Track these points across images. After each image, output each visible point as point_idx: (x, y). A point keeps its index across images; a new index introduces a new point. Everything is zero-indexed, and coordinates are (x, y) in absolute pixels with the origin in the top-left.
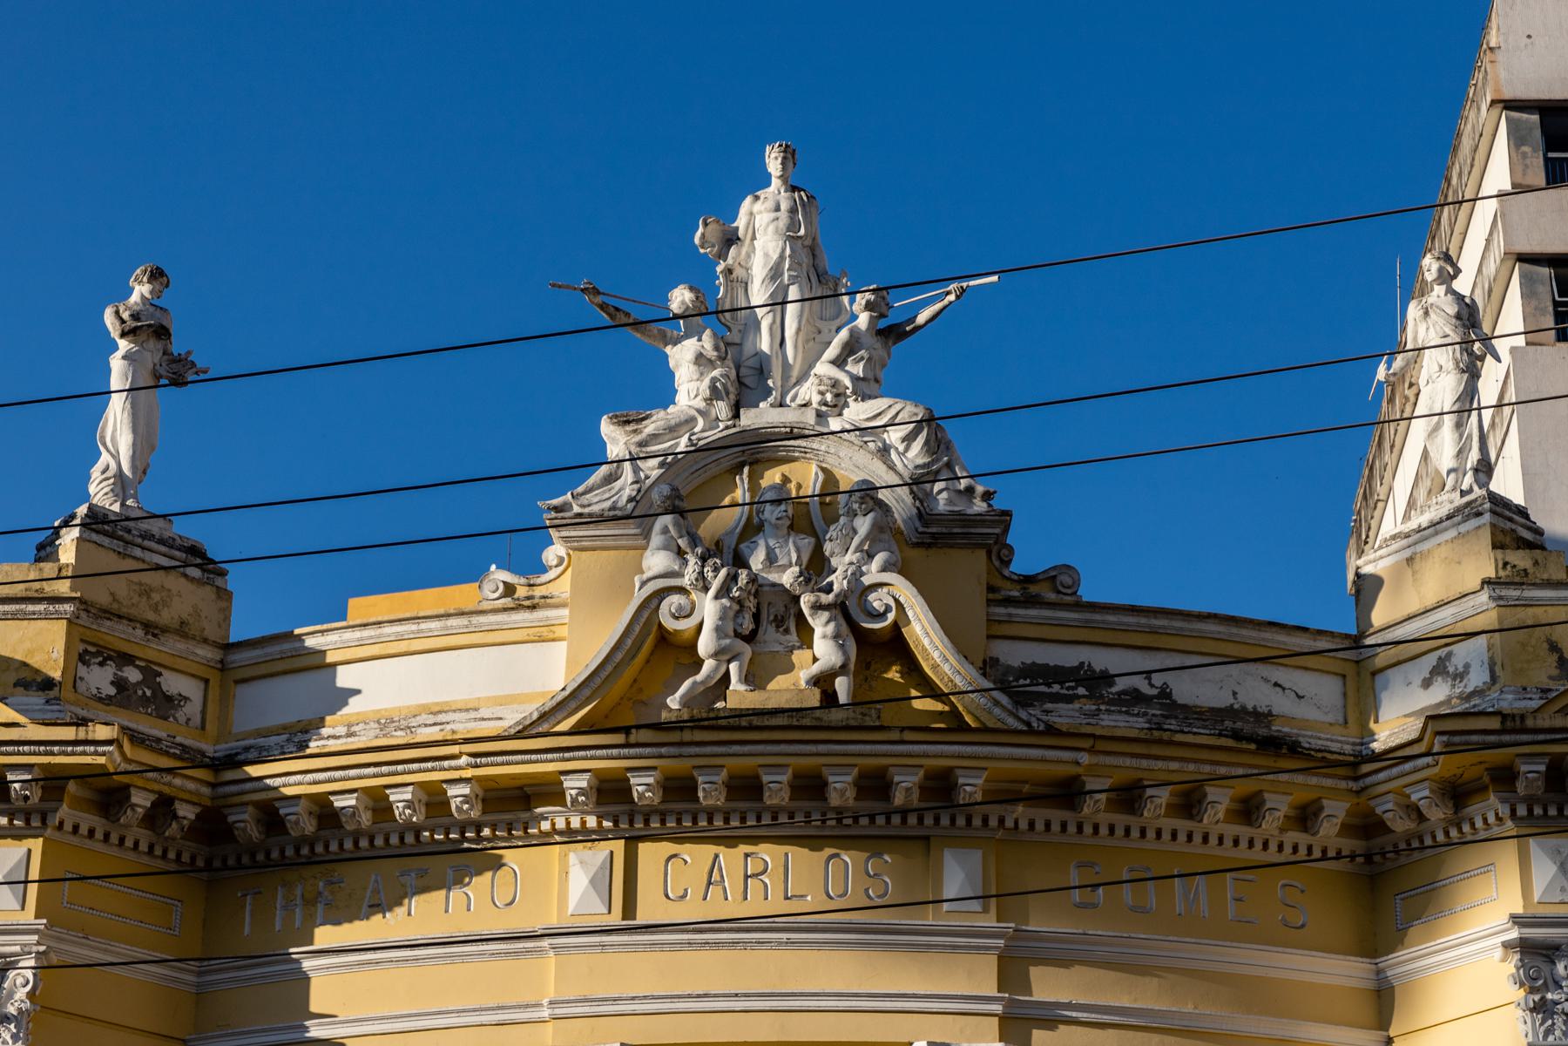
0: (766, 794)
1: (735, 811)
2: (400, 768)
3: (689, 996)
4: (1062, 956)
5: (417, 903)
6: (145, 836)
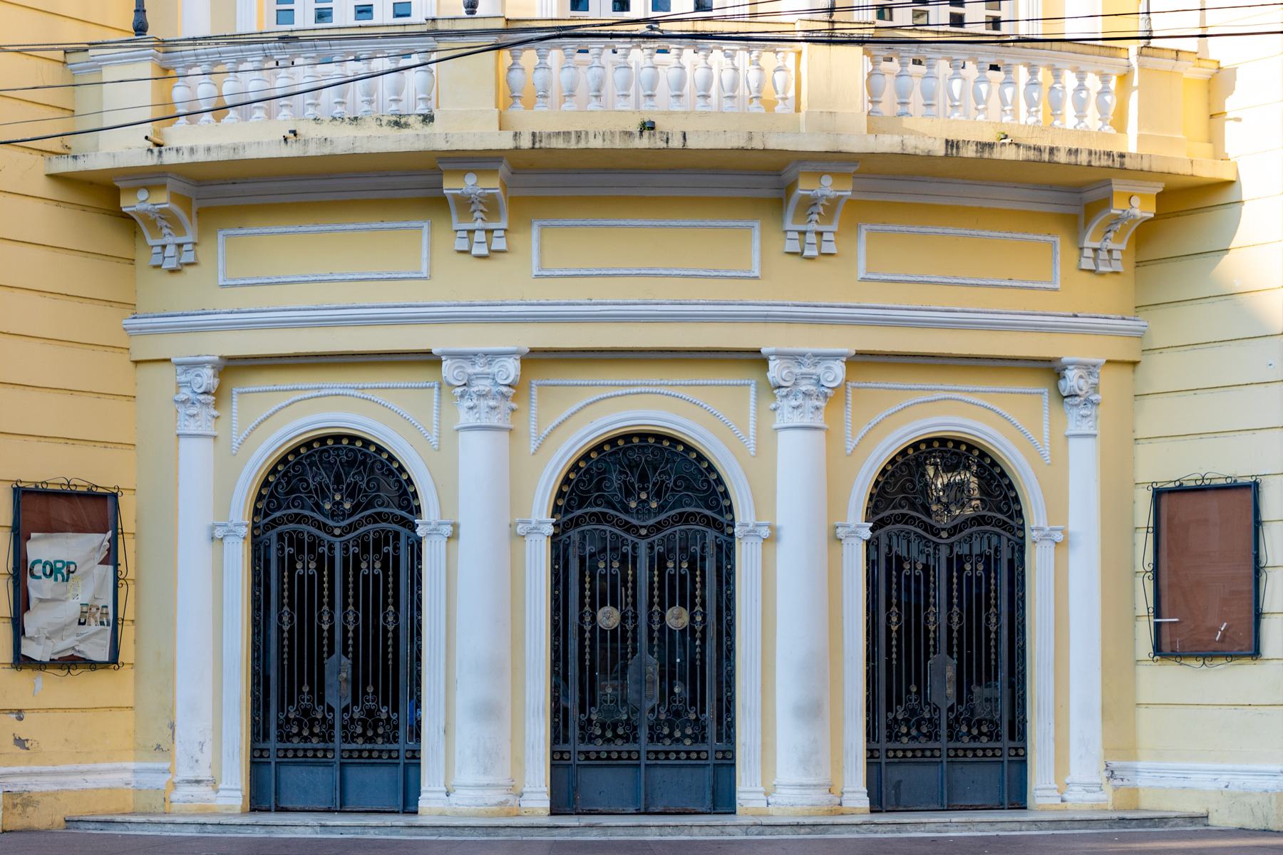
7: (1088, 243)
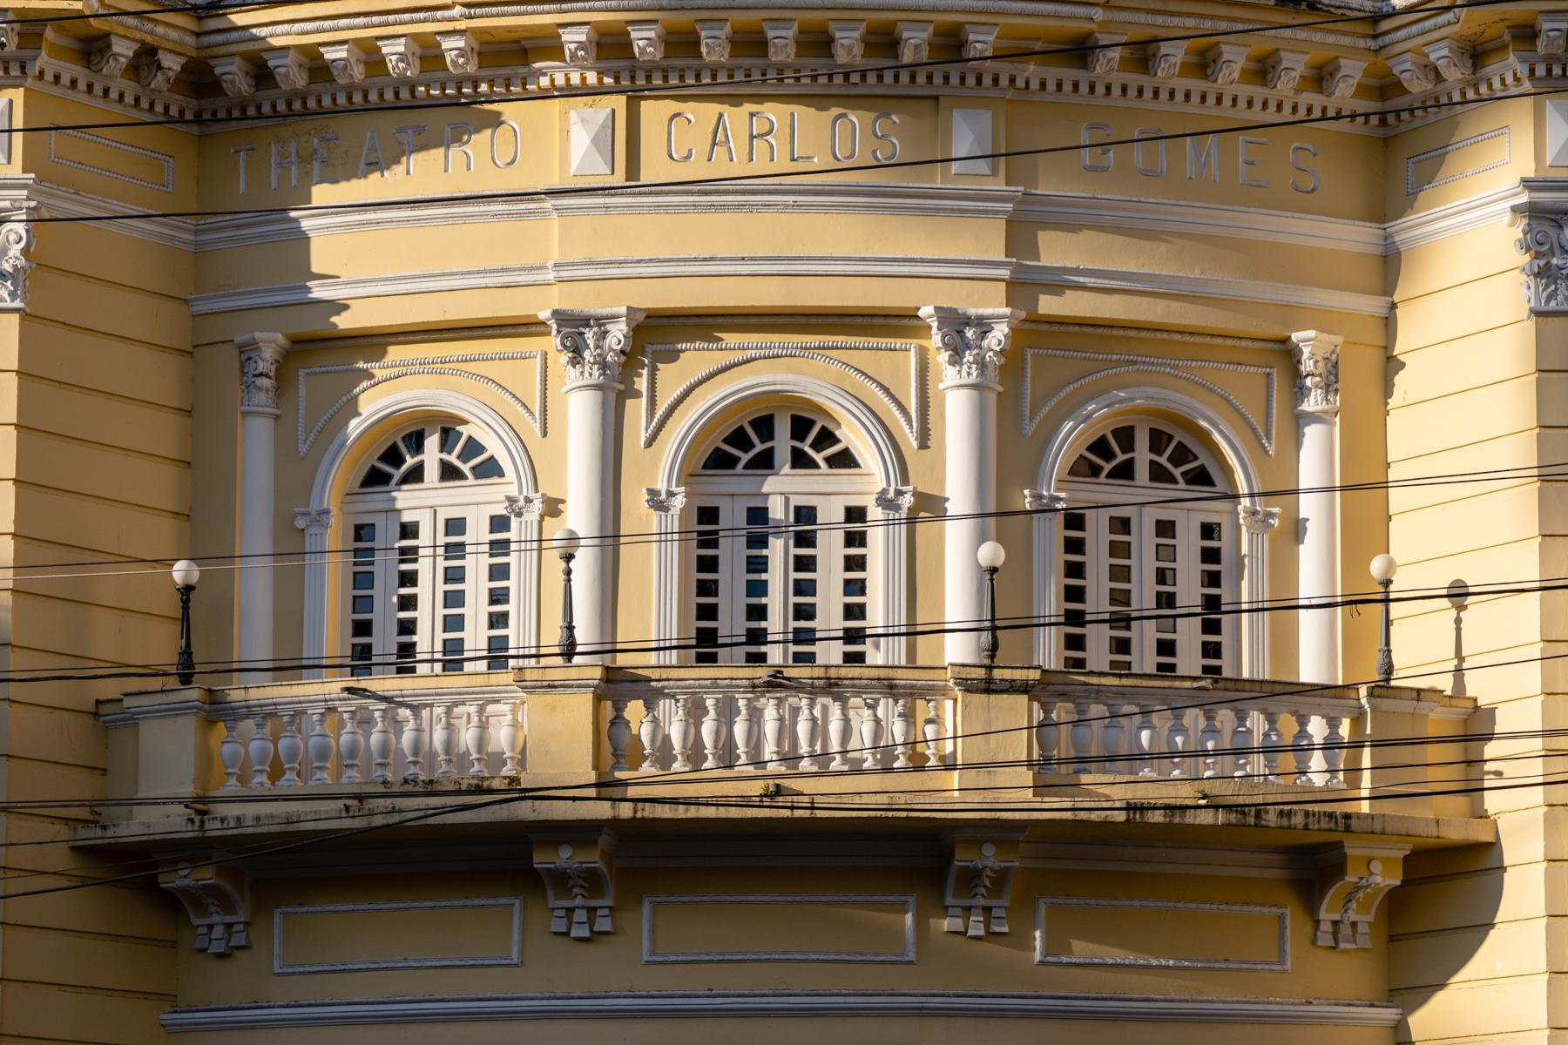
0: (772, 50)
1: (739, 68)
2: (391, 18)
3: (695, 259)
4: (1069, 220)
5: (416, 160)
6: (131, 89)
7: (1326, 915)
